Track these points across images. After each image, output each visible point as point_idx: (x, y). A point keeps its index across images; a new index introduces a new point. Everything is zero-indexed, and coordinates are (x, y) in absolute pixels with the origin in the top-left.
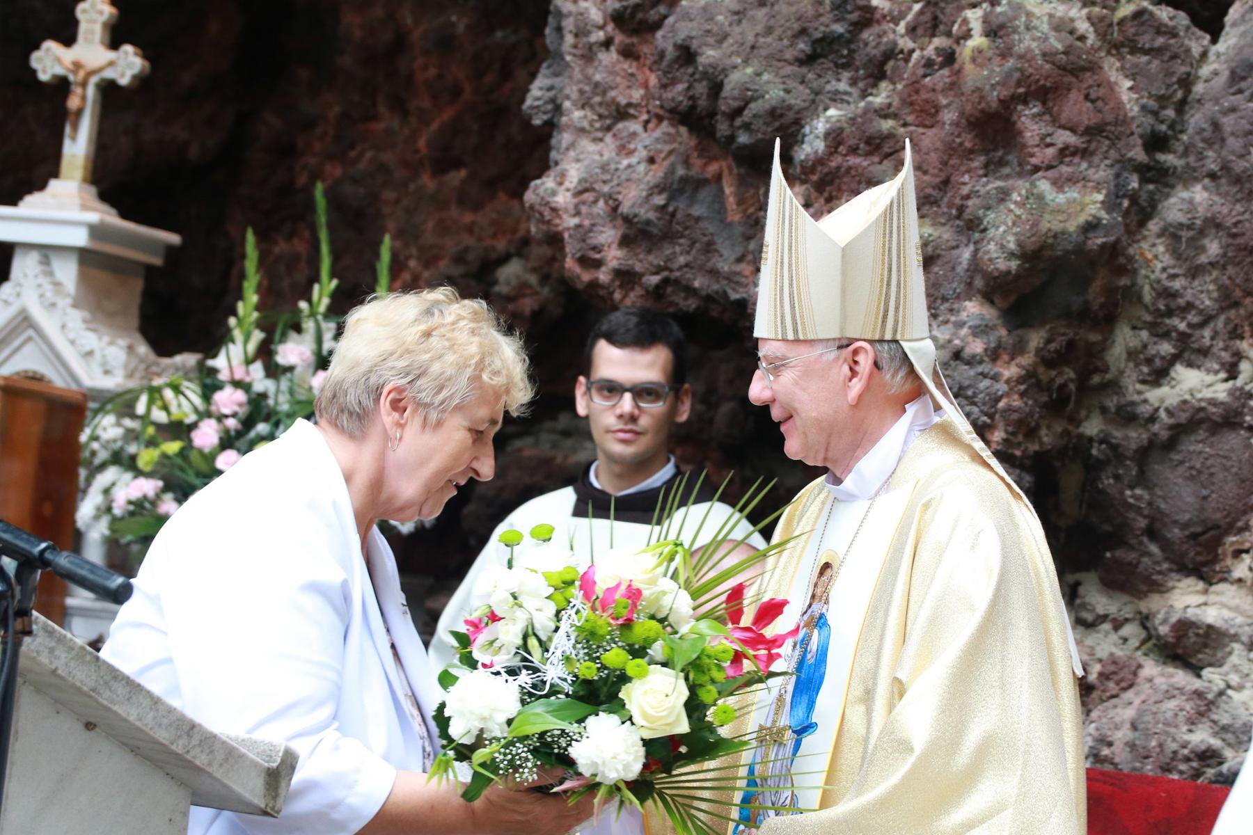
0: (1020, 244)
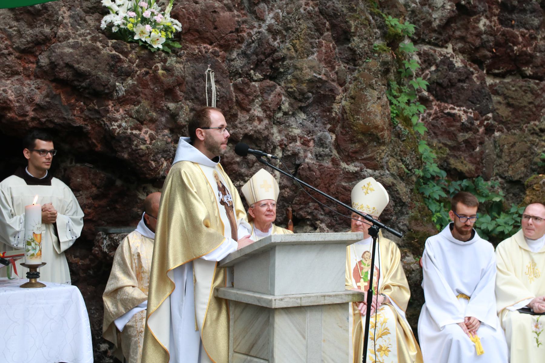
0: (189, 119)
